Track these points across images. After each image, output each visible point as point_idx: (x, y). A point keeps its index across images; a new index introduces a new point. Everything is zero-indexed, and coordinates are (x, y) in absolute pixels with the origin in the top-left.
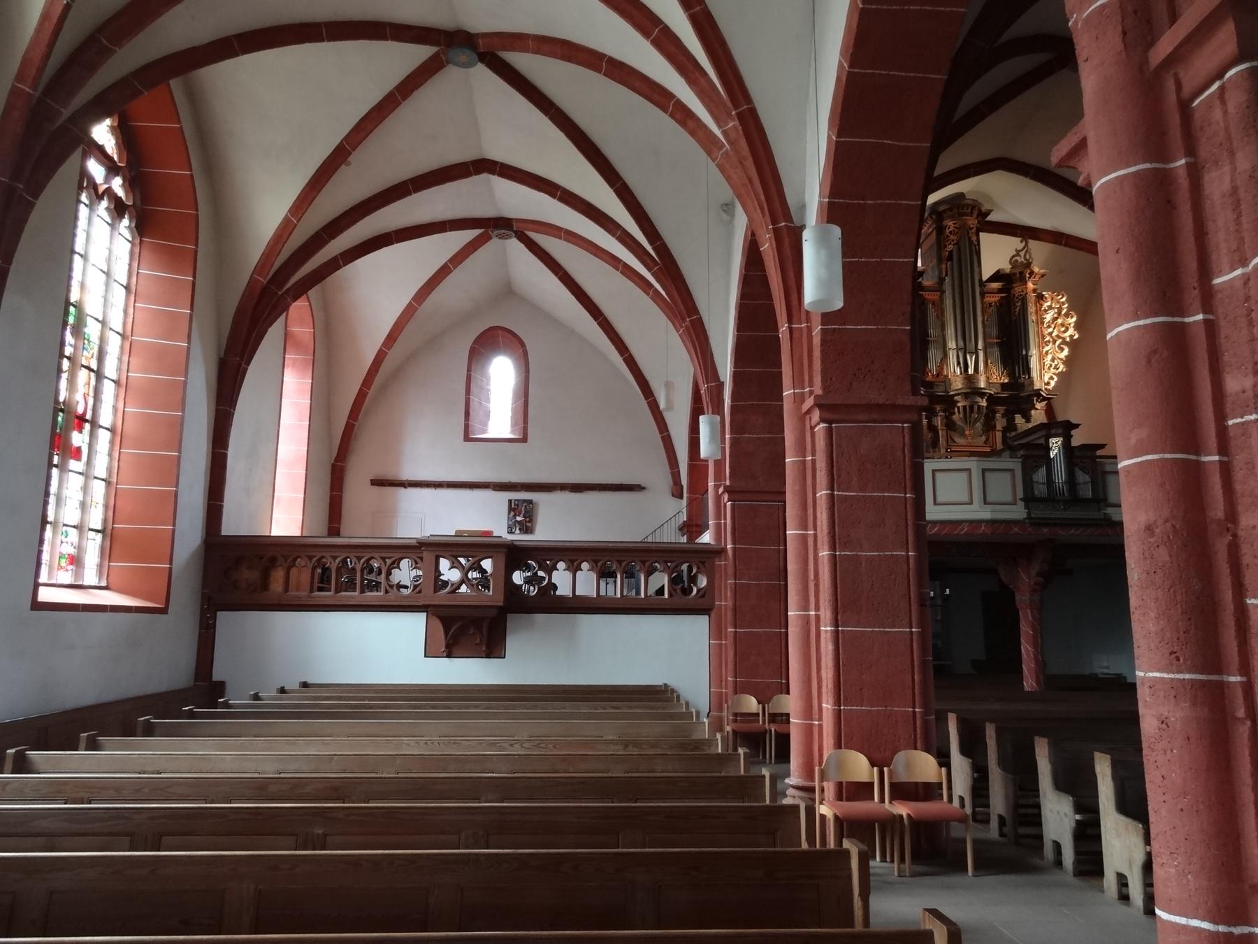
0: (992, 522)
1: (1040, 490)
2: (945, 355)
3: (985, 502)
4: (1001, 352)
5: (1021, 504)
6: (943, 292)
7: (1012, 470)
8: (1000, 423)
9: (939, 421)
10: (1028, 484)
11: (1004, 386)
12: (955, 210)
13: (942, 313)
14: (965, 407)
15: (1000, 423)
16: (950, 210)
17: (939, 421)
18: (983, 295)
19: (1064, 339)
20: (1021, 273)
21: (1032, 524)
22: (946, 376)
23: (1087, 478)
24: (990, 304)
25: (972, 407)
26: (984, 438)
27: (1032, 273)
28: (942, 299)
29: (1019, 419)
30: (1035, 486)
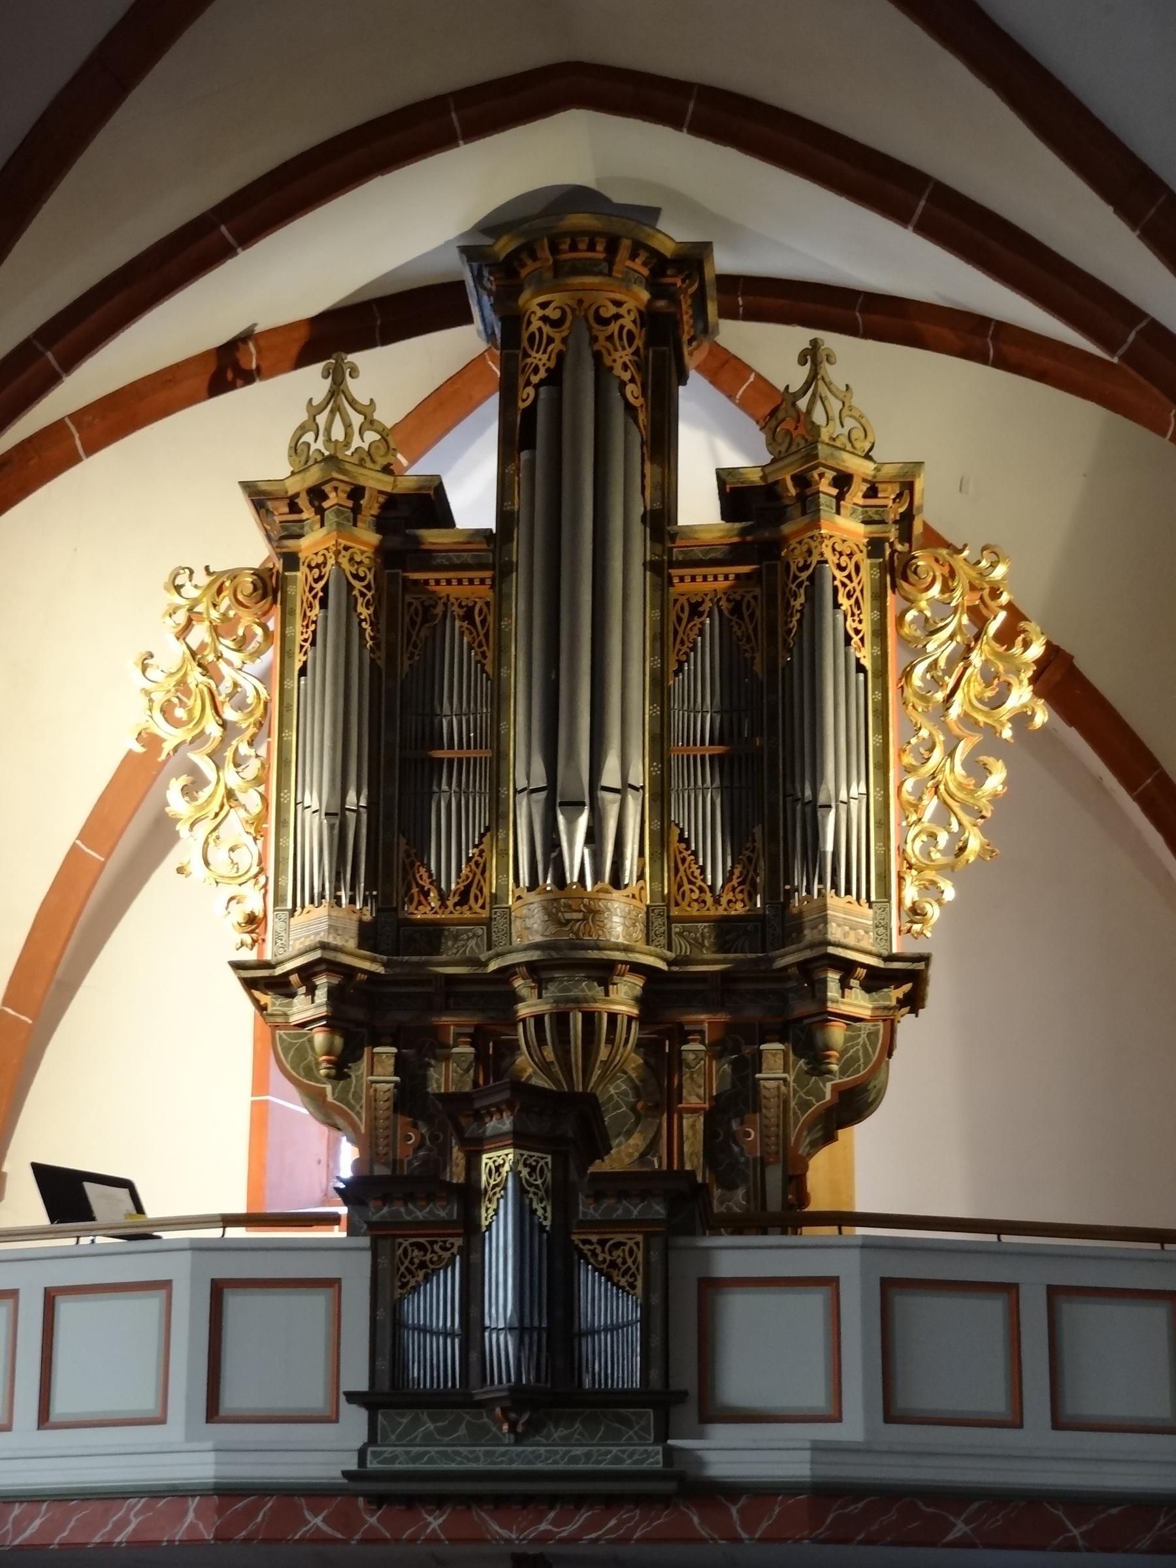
0: (226, 1493)
1: (433, 1359)
2: (498, 816)
3: (213, 1413)
4: (727, 791)
5: (355, 1420)
6: (502, 572)
7: (332, 1284)
8: (701, 1080)
10: (389, 1332)
11: (727, 932)
12: (545, 253)
13: (501, 651)
14: (539, 1019)
15: (701, 1080)
16: (529, 249)
18: (658, 569)
20: (802, 481)
21: (378, 1500)
23: (628, 1309)
24: (695, 609)
25: (561, 1020)
27: (843, 481)
28: (502, 599)
29: (776, 1064)
30: (412, 1341)
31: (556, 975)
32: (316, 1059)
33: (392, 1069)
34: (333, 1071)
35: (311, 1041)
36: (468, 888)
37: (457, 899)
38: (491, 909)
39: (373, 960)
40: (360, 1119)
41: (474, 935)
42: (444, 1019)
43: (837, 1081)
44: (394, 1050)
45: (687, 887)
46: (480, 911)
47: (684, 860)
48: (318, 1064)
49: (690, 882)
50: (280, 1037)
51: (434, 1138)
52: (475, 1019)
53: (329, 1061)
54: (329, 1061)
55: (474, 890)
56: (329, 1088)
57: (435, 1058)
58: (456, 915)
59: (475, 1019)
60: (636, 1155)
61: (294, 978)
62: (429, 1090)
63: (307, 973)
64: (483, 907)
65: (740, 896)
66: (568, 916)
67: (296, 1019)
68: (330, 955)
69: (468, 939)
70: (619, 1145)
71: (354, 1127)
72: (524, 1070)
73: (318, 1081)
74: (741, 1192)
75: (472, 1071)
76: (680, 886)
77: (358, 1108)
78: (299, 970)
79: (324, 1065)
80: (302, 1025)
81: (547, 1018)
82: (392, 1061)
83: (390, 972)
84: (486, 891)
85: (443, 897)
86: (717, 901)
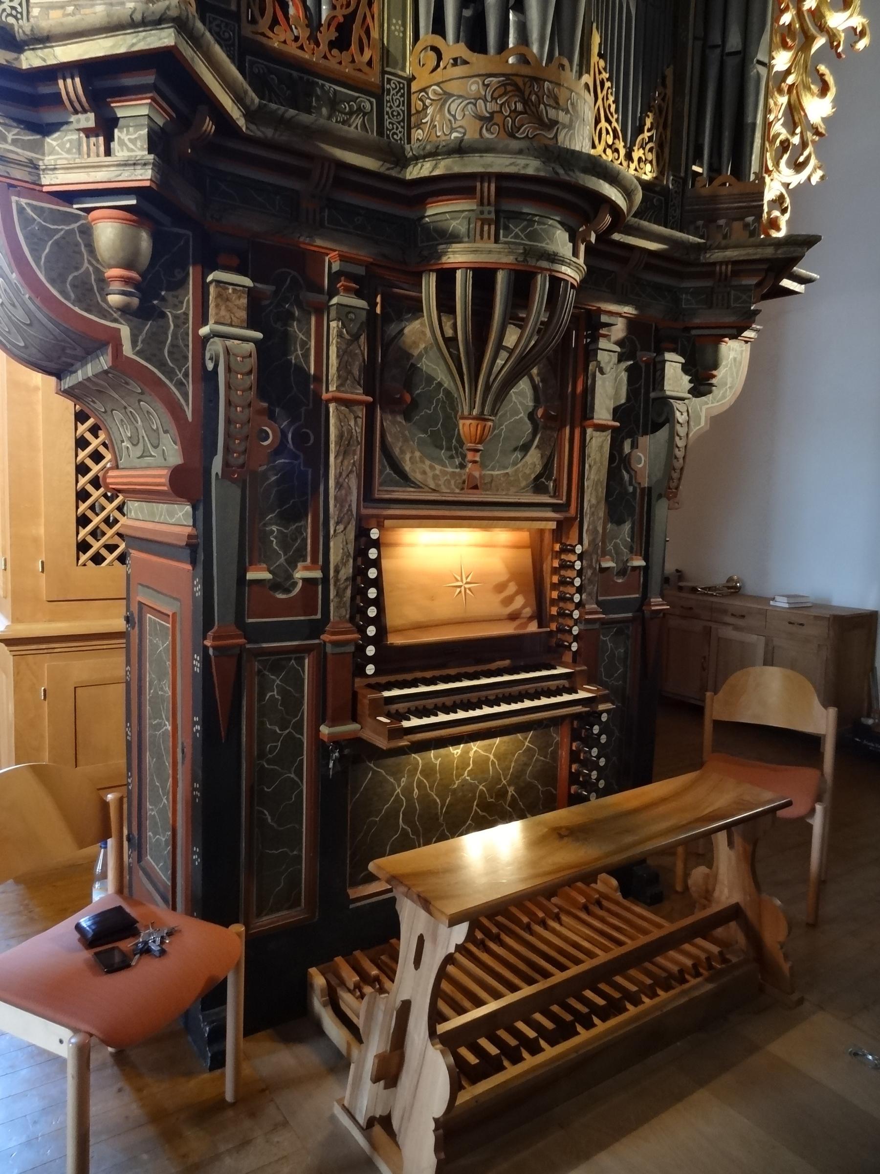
9: (328, 348)
14: (483, 278)
17: (328, 348)
19: (832, 36)
22: (388, 57)
26: (534, 459)
31: (525, 210)
32: (98, 271)
33: (243, 314)
34: (135, 301)
35: (87, 232)
36: (350, 18)
37: (333, 35)
38: (384, 72)
39: (239, 99)
40: (185, 395)
41: (360, 110)
42: (319, 242)
43: (710, 405)
44: (247, 282)
45: (603, 124)
46: (366, 69)
47: (602, 84)
48: (103, 281)
49: (608, 120)
50: (21, 210)
51: (300, 438)
52: (364, 254)
53: (127, 281)
54: (127, 281)
55: (357, 30)
56: (125, 331)
57: (300, 305)
58: (332, 63)
59: (364, 254)
60: (533, 476)
61: (71, 87)
62: (293, 358)
63: (104, 81)
64: (370, 63)
65: (650, 156)
66: (552, 113)
67: (52, 180)
68: (188, 52)
69: (351, 113)
70: (515, 464)
71: (175, 411)
72: (415, 344)
73: (104, 313)
74: (627, 527)
75: (363, 339)
76: (597, 121)
77: (180, 376)
78: (89, 70)
79: (116, 286)
80: (68, 197)
81: (501, 277)
82: (244, 301)
83: (257, 132)
84: (375, 34)
85: (313, 22)
86: (629, 157)
